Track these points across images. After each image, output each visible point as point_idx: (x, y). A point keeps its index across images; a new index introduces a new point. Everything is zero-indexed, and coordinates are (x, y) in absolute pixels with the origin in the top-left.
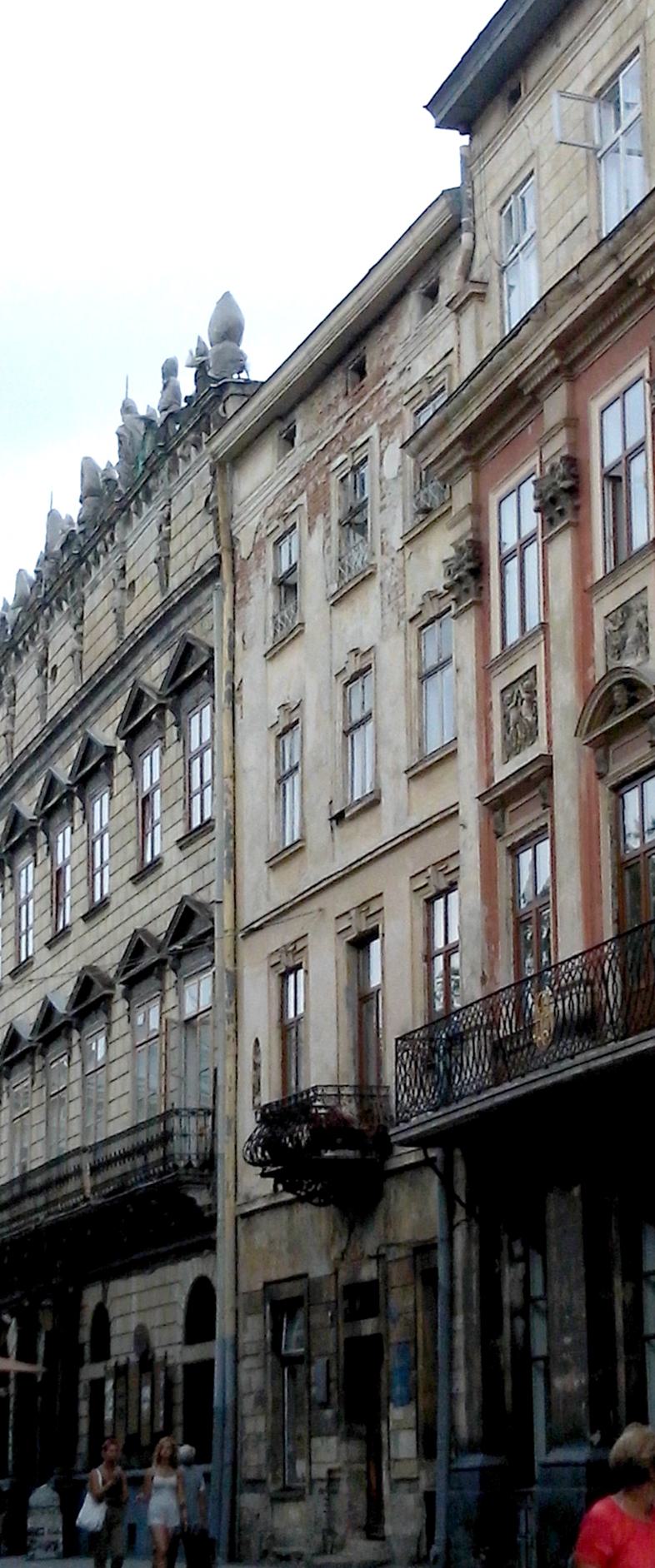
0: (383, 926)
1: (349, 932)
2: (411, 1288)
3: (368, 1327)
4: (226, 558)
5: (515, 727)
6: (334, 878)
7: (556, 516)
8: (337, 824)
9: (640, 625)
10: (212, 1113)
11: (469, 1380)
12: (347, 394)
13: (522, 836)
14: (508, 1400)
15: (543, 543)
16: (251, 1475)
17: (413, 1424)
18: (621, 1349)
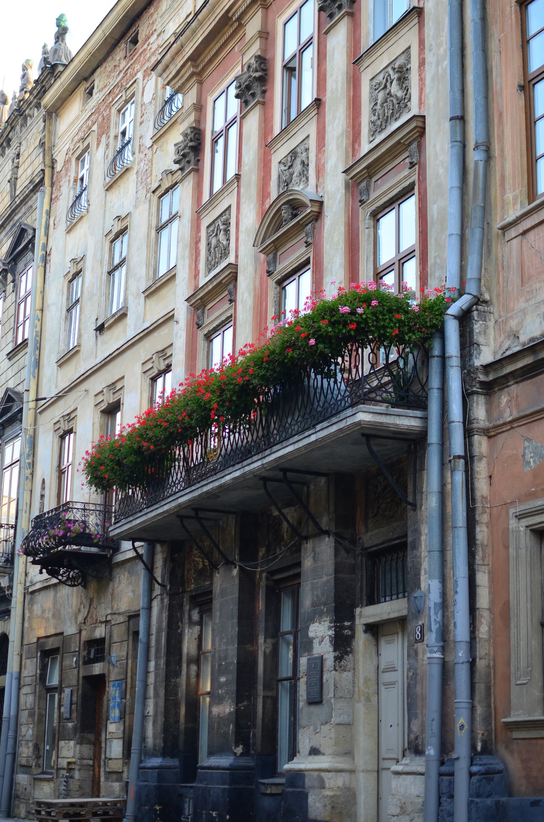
0: (123, 399)
1: (102, 404)
2: (125, 643)
3: (97, 669)
4: (48, 172)
5: (215, 250)
6: (95, 368)
7: (249, 98)
8: (100, 333)
9: (303, 163)
10: (15, 527)
11: (156, 705)
12: (126, 57)
13: (214, 325)
14: (182, 719)
15: (241, 118)
16: (24, 762)
17: (121, 735)
18: (260, 687)
